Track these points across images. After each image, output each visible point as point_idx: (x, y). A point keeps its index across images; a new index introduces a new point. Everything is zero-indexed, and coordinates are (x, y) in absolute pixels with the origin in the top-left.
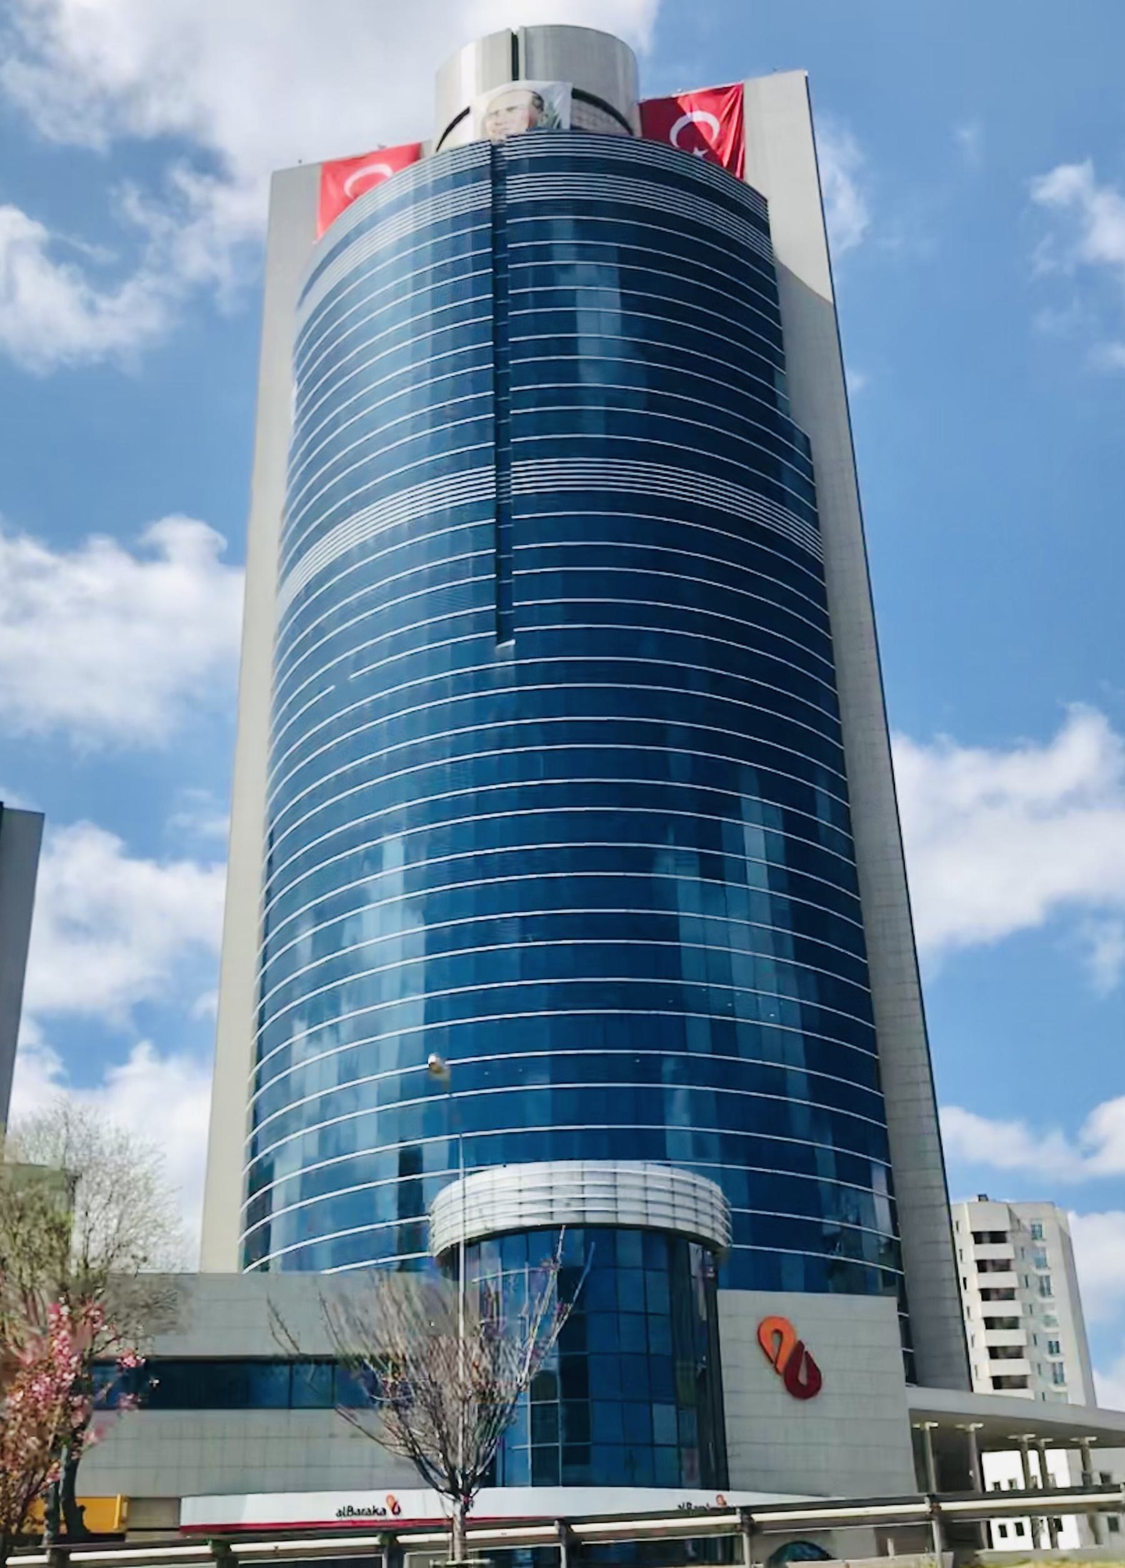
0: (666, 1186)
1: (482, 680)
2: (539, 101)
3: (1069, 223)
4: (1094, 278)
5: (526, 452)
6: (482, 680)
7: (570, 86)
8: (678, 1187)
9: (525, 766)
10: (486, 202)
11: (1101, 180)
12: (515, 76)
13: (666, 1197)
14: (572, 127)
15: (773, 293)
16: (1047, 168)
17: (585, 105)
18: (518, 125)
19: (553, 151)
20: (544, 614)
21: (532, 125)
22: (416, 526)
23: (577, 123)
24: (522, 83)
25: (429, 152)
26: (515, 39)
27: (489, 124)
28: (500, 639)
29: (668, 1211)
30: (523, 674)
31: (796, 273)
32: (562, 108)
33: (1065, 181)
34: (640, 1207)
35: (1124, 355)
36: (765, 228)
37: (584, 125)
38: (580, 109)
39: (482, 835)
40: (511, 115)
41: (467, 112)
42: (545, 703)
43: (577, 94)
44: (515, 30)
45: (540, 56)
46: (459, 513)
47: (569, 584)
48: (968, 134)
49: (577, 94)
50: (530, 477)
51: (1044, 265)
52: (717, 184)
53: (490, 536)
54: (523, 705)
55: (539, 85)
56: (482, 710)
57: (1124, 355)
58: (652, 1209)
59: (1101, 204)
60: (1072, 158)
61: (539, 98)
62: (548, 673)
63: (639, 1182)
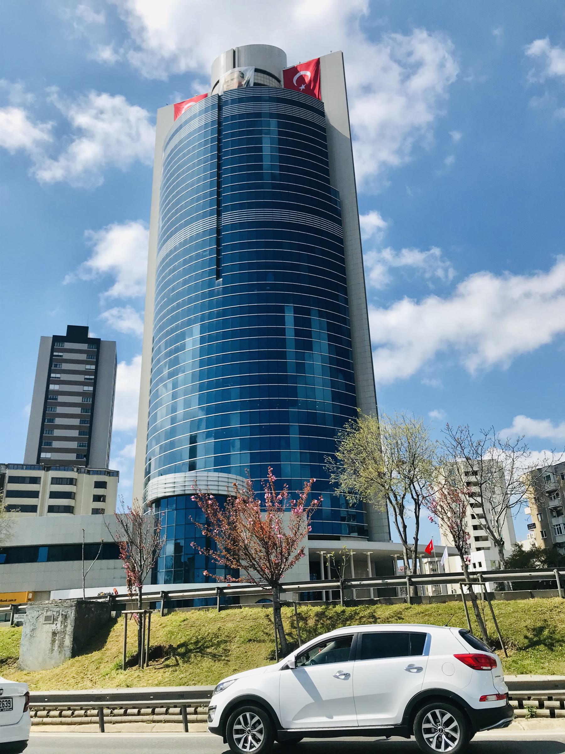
0: (216, 479)
1: (211, 294)
2: (242, 75)
3: (542, 61)
4: (554, 83)
5: (227, 209)
6: (211, 294)
7: (254, 67)
8: (220, 479)
9: (225, 324)
10: (216, 118)
11: (553, 43)
12: (234, 67)
13: (216, 483)
14: (255, 84)
15: (324, 138)
16: (531, 42)
17: (259, 74)
18: (235, 86)
19: (247, 94)
20: (232, 268)
21: (240, 85)
22: (198, 236)
23: (256, 81)
24: (237, 69)
25: (209, 96)
26: (234, 52)
27: (225, 86)
28: (217, 278)
29: (216, 488)
30: (225, 291)
31: (335, 127)
32: (250, 75)
33: (538, 46)
34: (216, 488)
35: (564, 113)
36: (322, 114)
37: (259, 82)
38: (257, 76)
39: (223, 348)
40: (232, 82)
41: (218, 82)
42: (233, 300)
43: (257, 70)
44: (234, 49)
45: (243, 58)
46: (204, 233)
47: (241, 256)
48: (497, 32)
49: (257, 70)
50: (228, 218)
51: (532, 80)
52: (302, 99)
53: (214, 241)
54: (224, 302)
55: (242, 69)
56: (210, 305)
57: (564, 113)
58: (220, 488)
59: (555, 53)
60: (541, 37)
61: (243, 74)
62: (233, 290)
63: (206, 478)
